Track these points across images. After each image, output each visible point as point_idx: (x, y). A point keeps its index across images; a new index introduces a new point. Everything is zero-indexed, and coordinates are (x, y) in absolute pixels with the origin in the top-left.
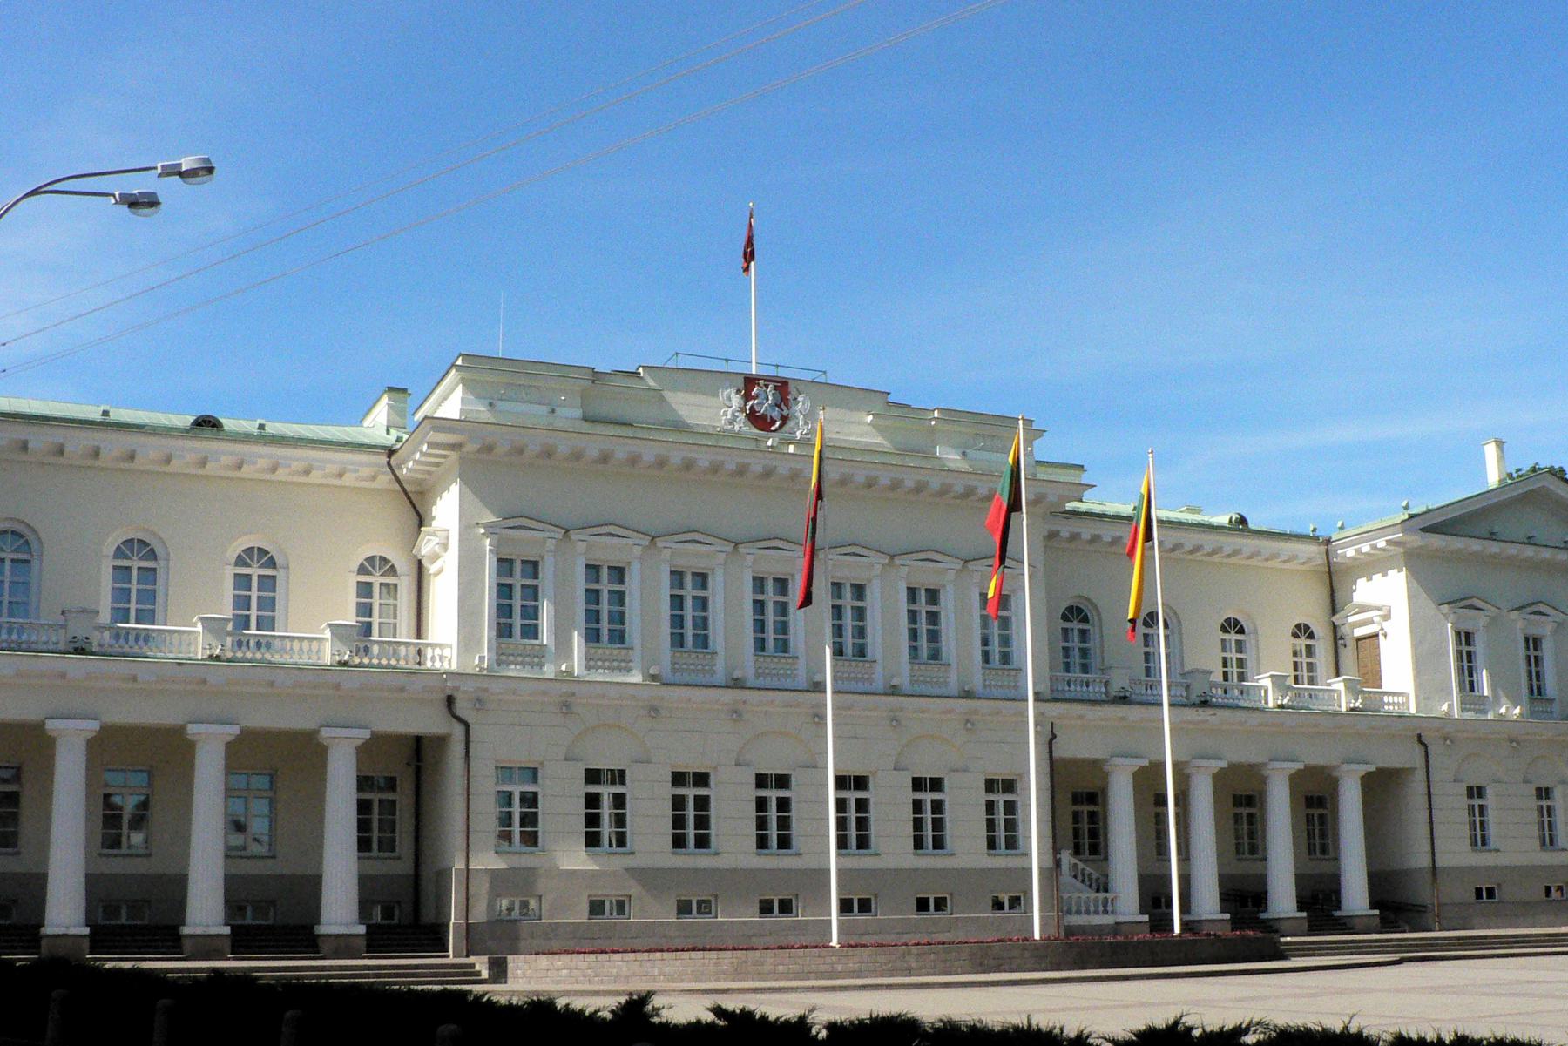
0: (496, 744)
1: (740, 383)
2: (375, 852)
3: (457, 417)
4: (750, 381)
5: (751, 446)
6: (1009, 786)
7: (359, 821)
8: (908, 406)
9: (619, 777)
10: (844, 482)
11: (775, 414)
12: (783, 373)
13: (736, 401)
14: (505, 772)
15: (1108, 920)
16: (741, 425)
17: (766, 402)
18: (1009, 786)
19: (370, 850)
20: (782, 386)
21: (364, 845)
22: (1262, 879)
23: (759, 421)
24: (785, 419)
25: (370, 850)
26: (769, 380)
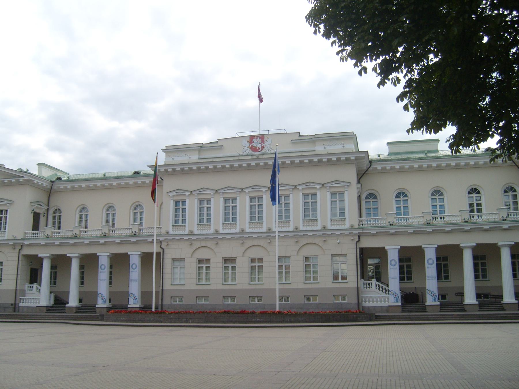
1: (248, 139)
2: (481, 279)
3: (163, 164)
4: (252, 138)
5: (250, 157)
7: (513, 268)
8: (307, 136)
10: (284, 163)
11: (260, 146)
12: (262, 133)
13: (248, 144)
16: (250, 152)
17: (257, 144)
19: (479, 278)
20: (262, 137)
21: (476, 276)
22: (463, 288)
23: (254, 149)
24: (263, 147)
25: (479, 278)
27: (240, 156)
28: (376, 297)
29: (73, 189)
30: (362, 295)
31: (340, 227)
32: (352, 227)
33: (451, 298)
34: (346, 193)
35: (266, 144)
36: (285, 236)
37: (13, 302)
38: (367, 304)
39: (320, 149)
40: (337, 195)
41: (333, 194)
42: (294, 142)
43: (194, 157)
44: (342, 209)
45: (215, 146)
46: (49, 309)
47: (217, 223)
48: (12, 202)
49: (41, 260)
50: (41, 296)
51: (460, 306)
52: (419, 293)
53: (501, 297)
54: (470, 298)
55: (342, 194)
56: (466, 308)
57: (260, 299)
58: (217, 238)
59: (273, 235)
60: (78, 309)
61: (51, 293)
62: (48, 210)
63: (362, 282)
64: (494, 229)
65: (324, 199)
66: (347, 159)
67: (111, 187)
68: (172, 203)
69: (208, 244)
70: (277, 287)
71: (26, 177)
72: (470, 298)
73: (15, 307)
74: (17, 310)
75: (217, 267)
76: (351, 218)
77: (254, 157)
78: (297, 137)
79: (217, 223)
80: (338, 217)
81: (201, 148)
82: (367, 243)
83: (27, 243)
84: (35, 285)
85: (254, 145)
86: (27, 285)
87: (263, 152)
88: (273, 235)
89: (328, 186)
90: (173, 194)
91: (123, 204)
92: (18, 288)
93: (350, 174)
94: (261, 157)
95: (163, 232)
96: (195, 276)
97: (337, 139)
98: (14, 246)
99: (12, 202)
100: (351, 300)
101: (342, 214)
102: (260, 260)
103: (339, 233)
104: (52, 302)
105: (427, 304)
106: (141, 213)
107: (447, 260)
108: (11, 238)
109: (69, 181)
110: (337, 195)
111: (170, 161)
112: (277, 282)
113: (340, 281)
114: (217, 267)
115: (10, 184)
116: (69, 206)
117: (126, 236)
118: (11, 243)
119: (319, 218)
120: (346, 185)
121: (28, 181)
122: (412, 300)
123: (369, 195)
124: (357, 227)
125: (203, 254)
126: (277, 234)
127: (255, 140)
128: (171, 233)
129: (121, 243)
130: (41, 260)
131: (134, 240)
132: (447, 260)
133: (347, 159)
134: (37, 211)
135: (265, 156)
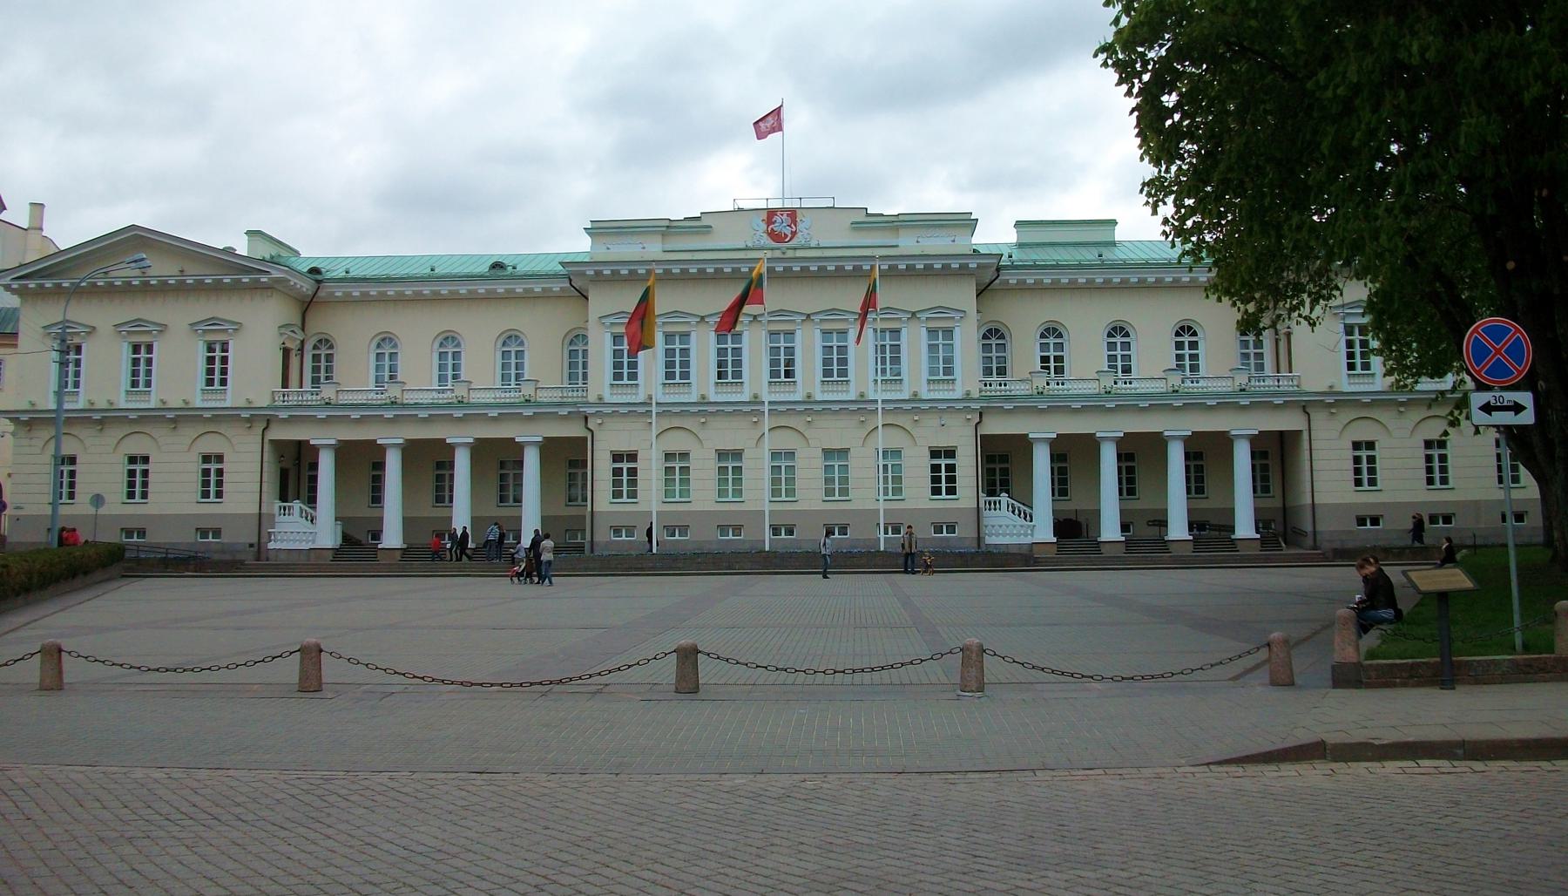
0: (607, 441)
1: (764, 215)
4: (771, 213)
6: (951, 453)
9: (632, 457)
11: (788, 231)
13: (764, 226)
14: (617, 457)
15: (1029, 540)
16: (767, 241)
17: (781, 225)
18: (951, 453)
20: (792, 213)
23: (777, 237)
24: (794, 234)
26: (783, 210)
27: (747, 249)
28: (1006, 527)
29: (365, 300)
30: (985, 522)
31: (947, 395)
32: (967, 398)
33: (1142, 531)
34: (957, 332)
35: (800, 226)
36: (895, 408)
37: (255, 540)
38: (990, 540)
39: (908, 243)
40: (941, 335)
41: (932, 332)
42: (857, 226)
43: (653, 249)
44: (948, 360)
45: (697, 226)
46: (336, 552)
47: (809, 380)
48: (238, 327)
49: (315, 450)
50: (317, 528)
51: (1162, 544)
52: (1081, 519)
53: (1232, 529)
54: (1178, 529)
55: (949, 333)
56: (1172, 547)
57: (790, 532)
58: (705, 410)
59: (870, 407)
60: (406, 552)
61: (336, 519)
62: (302, 342)
63: (983, 497)
64: (1225, 404)
65: (914, 341)
66: (964, 267)
67: (454, 299)
68: (608, 339)
69: (687, 423)
70: (882, 506)
71: (276, 274)
72: (1178, 529)
73: (259, 549)
74: (263, 556)
75: (704, 468)
76: (968, 377)
77: (778, 254)
78: (862, 218)
79: (809, 380)
80: (942, 377)
81: (668, 228)
82: (997, 426)
83: (283, 415)
84: (297, 505)
85: (776, 227)
86: (278, 504)
87: (794, 243)
88: (870, 407)
89: (923, 316)
90: (608, 321)
91: (480, 338)
92: (264, 510)
93: (963, 296)
94: (790, 254)
95: (592, 398)
96: (713, 485)
97: (942, 226)
98: (251, 420)
99: (238, 327)
100: (965, 532)
101: (948, 371)
102: (685, 456)
103: (944, 406)
104: (339, 541)
105: (1103, 539)
106: (519, 354)
107: (1065, 460)
108: (242, 404)
109: (347, 280)
110: (941, 335)
111: (603, 254)
112: (881, 497)
113: (944, 495)
114: (704, 468)
115: (236, 288)
116: (353, 339)
117: (511, 405)
118: (245, 415)
119: (905, 376)
120: (957, 316)
121: (278, 280)
122: (1073, 530)
123: (990, 331)
124: (977, 395)
125: (677, 443)
126: (880, 406)
127: (777, 219)
128: (608, 398)
129: (430, 419)
130: (382, 449)
131: (528, 412)
132: (1065, 460)
133: (964, 267)
134: (288, 345)
135: (800, 254)
